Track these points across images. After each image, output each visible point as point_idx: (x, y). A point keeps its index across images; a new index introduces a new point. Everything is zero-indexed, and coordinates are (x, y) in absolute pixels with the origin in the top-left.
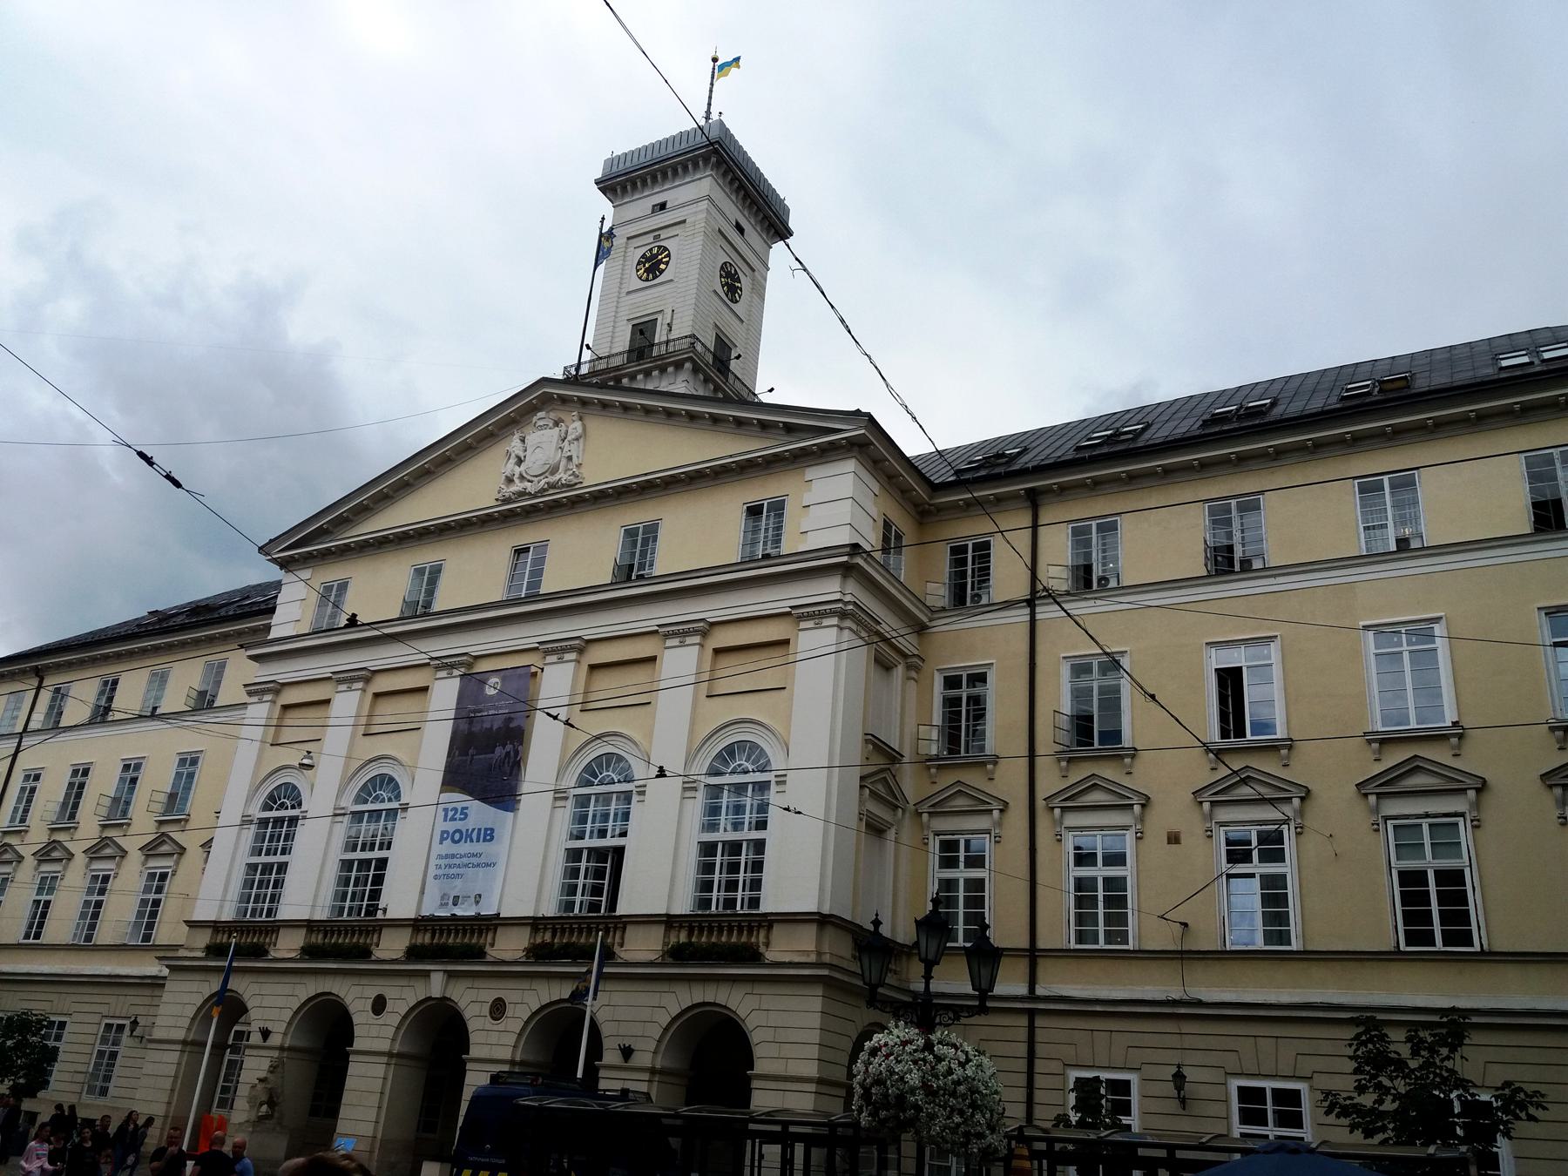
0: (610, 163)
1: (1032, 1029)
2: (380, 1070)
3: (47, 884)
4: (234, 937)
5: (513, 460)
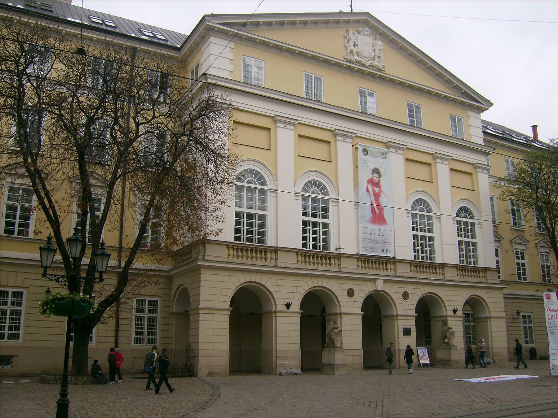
5: (351, 44)
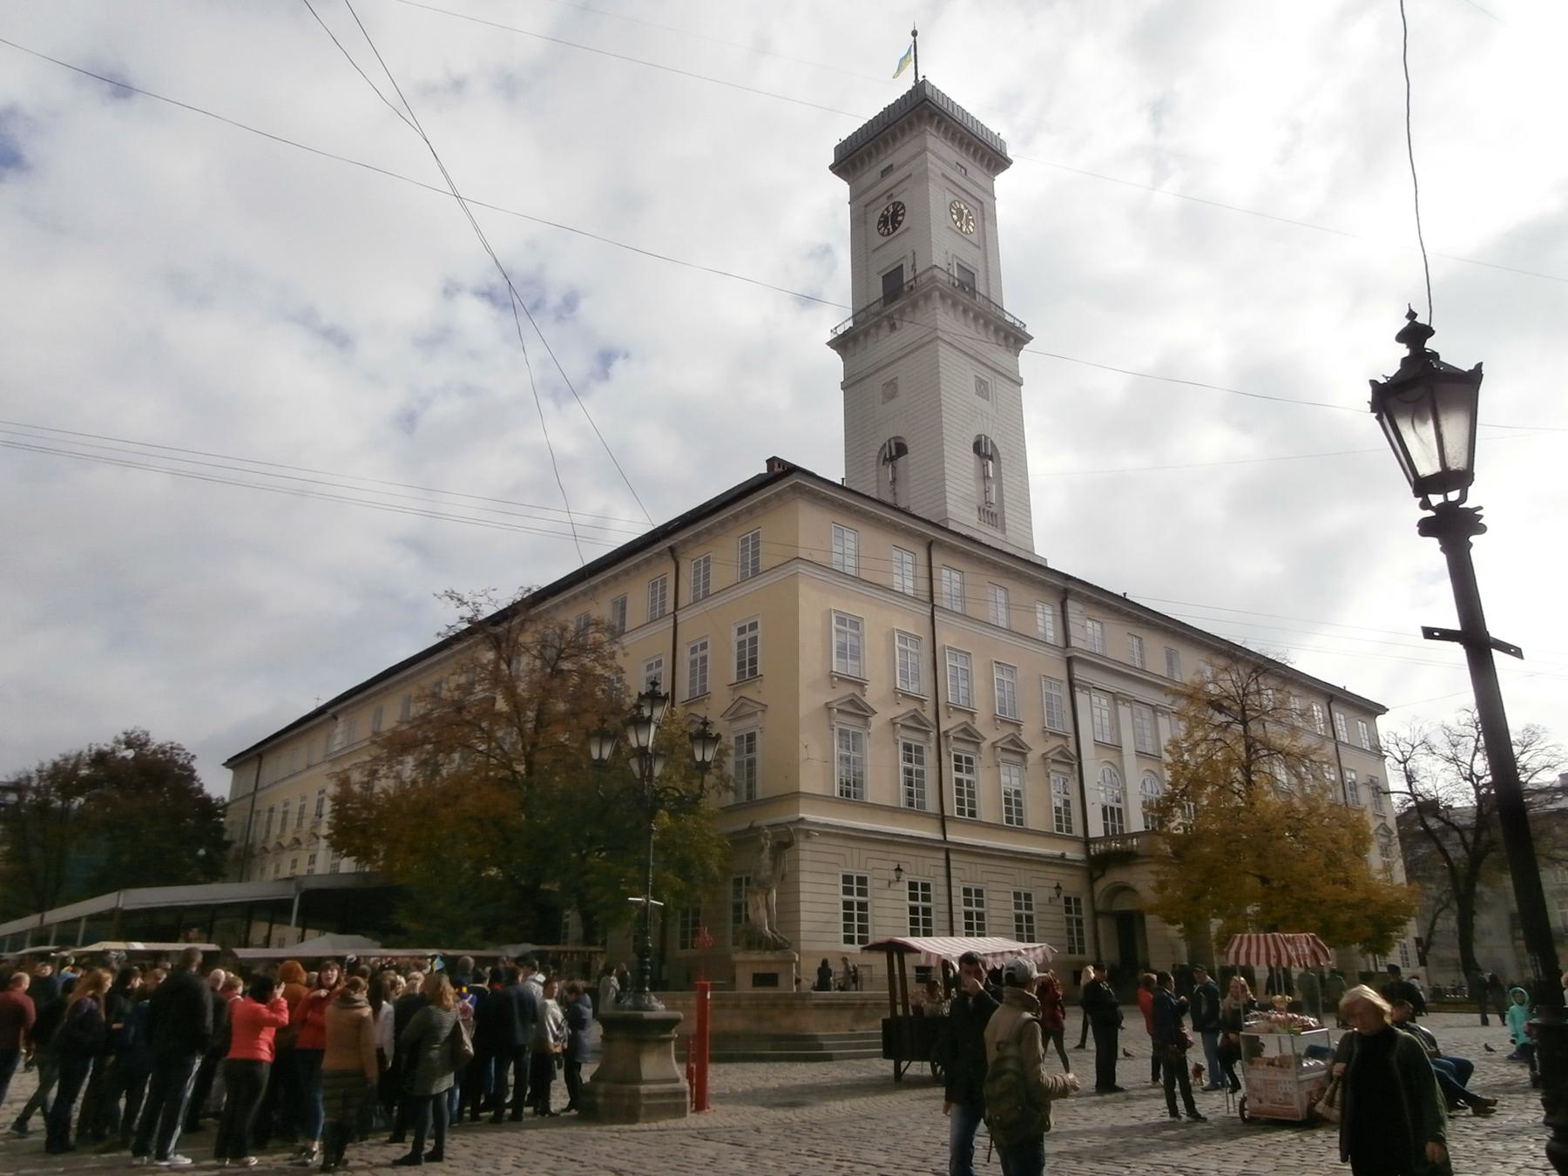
0: (838, 149)
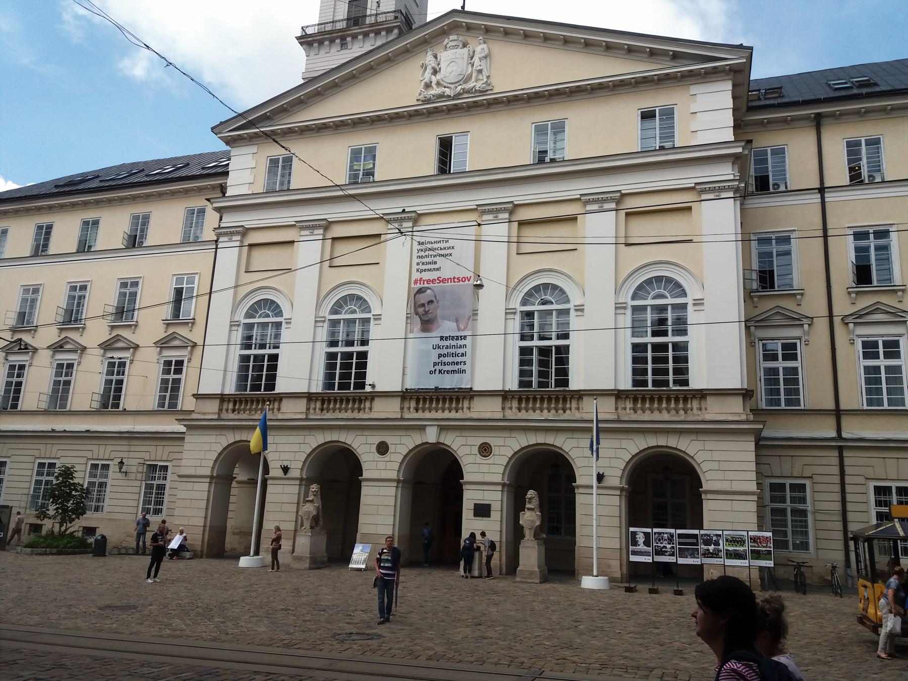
1: (841, 458)
2: (392, 491)
3: (117, 368)
4: (268, 405)
5: (429, 71)
